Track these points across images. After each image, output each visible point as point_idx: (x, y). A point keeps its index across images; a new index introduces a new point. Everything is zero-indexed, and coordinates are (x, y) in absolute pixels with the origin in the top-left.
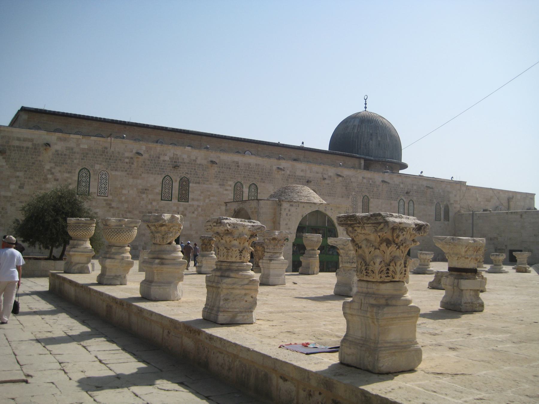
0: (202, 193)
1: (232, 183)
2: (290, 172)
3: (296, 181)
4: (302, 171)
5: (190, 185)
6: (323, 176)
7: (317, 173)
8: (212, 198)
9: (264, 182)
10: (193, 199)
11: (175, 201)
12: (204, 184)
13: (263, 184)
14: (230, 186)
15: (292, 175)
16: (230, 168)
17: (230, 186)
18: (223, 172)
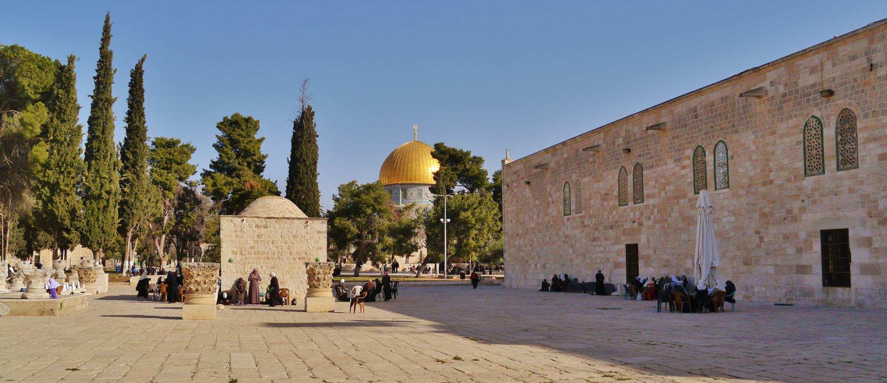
0: (656, 182)
1: (689, 152)
2: (786, 85)
3: (799, 104)
4: (813, 71)
5: (644, 172)
6: (869, 60)
7: (853, 58)
8: (667, 188)
9: (736, 132)
10: (648, 196)
11: (631, 204)
12: (658, 166)
13: (735, 137)
14: (688, 158)
15: (791, 93)
16: (686, 126)
17: (688, 158)
18: (677, 137)
